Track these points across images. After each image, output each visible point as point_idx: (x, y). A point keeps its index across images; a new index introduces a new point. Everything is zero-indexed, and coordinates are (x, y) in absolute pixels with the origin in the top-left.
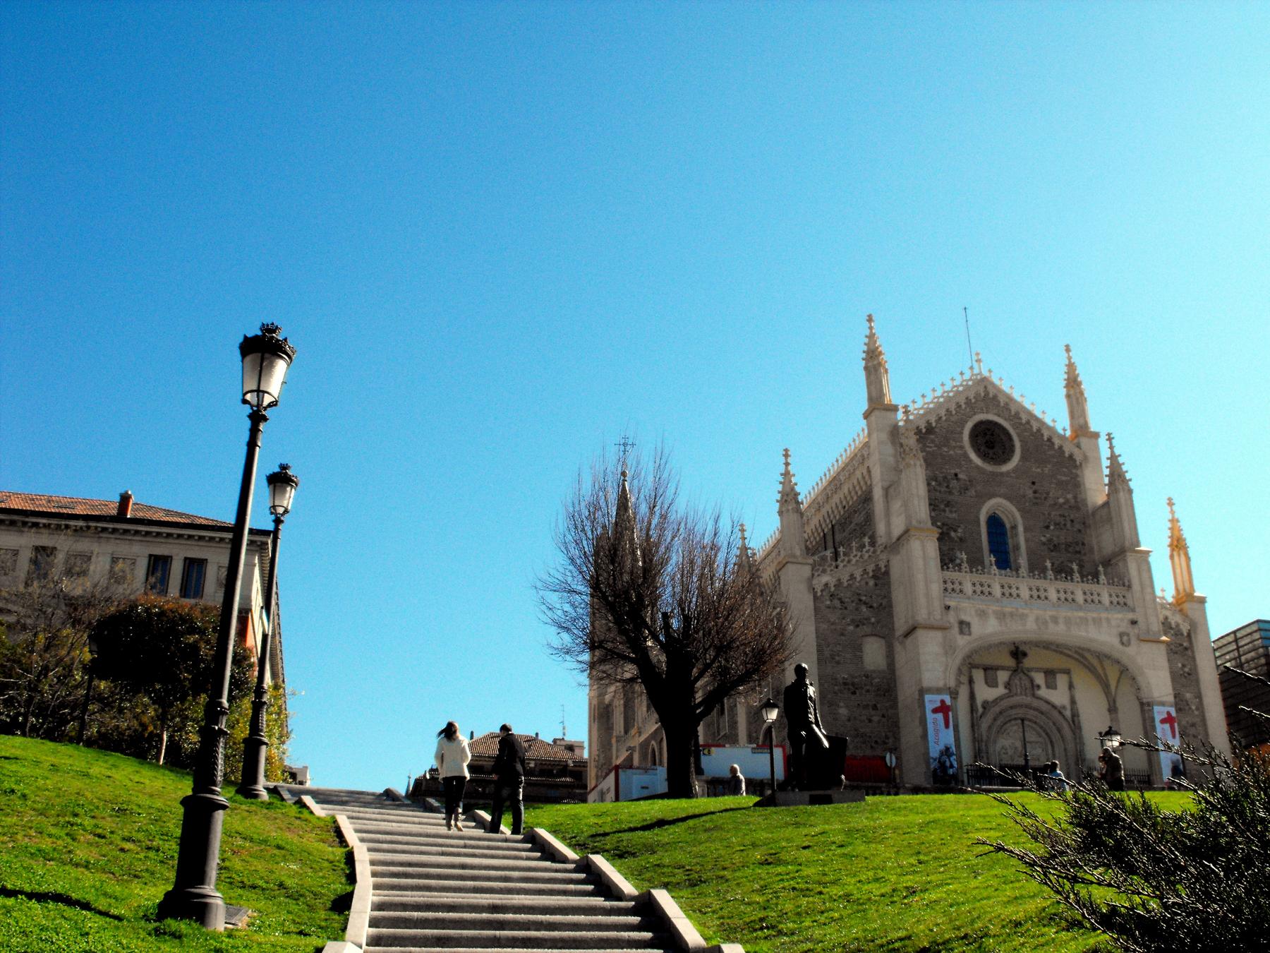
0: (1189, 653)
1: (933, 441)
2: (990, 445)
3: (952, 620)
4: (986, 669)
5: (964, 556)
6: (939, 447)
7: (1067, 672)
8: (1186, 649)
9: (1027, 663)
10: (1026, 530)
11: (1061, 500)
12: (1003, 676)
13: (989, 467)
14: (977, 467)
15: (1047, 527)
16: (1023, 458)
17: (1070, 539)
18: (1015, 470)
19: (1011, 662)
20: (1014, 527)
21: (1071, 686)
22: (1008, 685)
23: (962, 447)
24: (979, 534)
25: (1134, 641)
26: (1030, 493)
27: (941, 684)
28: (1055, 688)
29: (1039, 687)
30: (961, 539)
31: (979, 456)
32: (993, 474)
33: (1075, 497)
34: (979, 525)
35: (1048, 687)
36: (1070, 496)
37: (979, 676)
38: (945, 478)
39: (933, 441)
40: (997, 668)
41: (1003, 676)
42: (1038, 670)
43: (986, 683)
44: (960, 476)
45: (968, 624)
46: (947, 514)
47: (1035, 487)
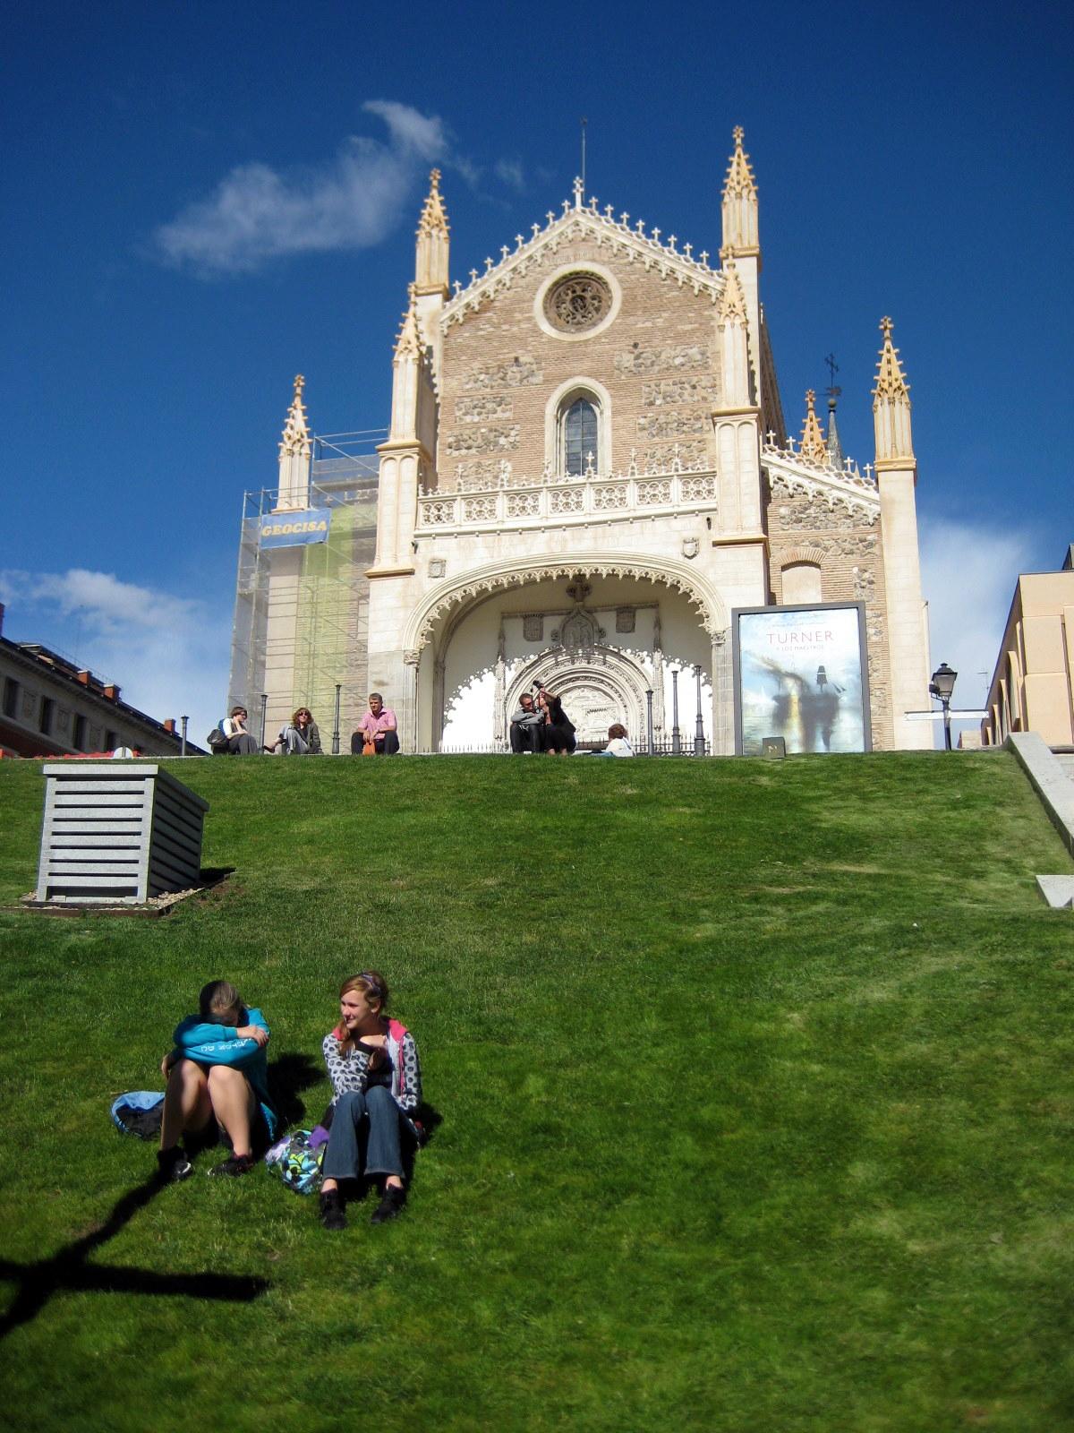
0: (875, 550)
1: (489, 321)
2: (579, 302)
3: (420, 560)
4: (525, 617)
5: (510, 469)
6: (497, 326)
7: (655, 605)
8: (871, 545)
9: (591, 601)
10: (615, 413)
11: (677, 361)
12: (551, 624)
13: (566, 337)
14: (551, 340)
15: (652, 404)
16: (625, 312)
17: (686, 413)
18: (606, 334)
19: (568, 602)
20: (601, 413)
21: (658, 624)
22: (555, 636)
23: (530, 319)
24: (542, 431)
25: (705, 546)
26: (628, 360)
27: (393, 648)
28: (632, 630)
29: (602, 633)
30: (514, 446)
31: (554, 325)
32: (572, 344)
33: (703, 354)
34: (543, 422)
35: (619, 630)
36: (694, 352)
37: (516, 628)
38: (500, 367)
39: (489, 321)
40: (542, 616)
41: (551, 624)
42: (606, 608)
43: (525, 636)
44: (522, 359)
45: (442, 563)
46: (500, 415)
47: (636, 352)
